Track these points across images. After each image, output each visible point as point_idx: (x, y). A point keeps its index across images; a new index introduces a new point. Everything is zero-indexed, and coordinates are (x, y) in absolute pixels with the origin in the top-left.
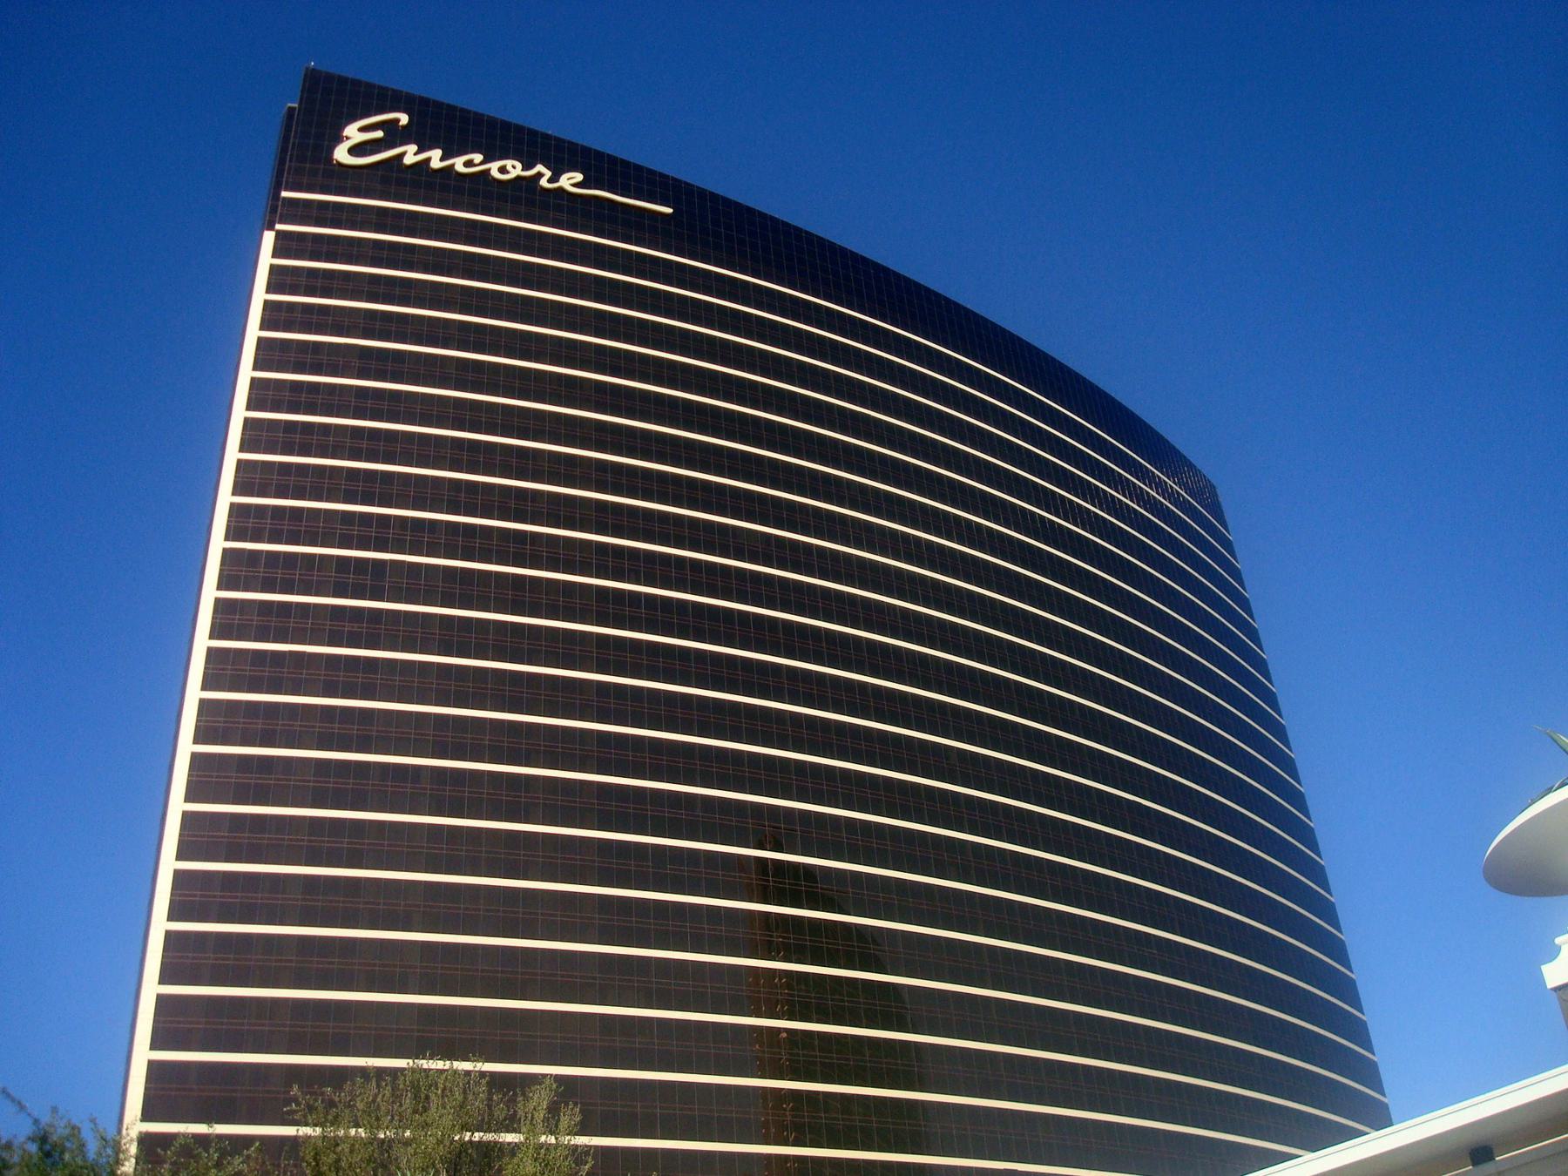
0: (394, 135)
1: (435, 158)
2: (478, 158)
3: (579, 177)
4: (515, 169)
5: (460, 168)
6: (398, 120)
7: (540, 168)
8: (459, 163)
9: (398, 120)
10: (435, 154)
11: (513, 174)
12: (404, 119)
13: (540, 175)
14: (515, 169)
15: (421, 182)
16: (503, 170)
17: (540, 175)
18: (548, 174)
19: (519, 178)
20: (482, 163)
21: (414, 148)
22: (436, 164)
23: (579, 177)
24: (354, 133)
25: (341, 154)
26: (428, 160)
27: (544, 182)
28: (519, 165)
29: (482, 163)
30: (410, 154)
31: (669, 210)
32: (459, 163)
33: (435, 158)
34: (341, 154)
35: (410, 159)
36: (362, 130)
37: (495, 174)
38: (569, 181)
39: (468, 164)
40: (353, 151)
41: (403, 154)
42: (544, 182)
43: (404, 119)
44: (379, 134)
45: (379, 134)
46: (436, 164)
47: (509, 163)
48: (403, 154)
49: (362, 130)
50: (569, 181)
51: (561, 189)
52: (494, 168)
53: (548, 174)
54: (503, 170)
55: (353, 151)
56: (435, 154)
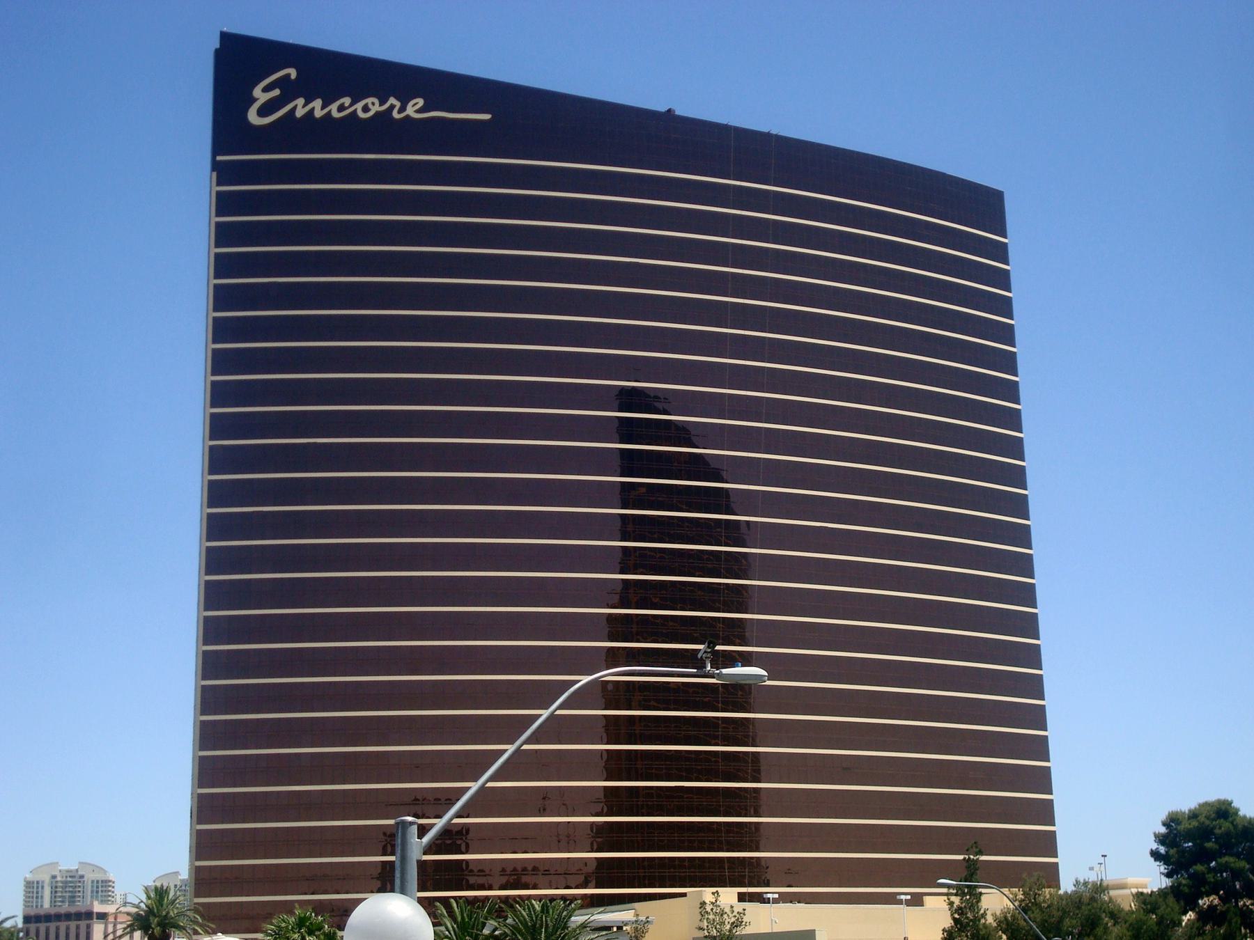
0: (289, 91)
2: (347, 101)
3: (420, 102)
4: (375, 106)
5: (336, 114)
6: (288, 75)
7: (392, 101)
8: (333, 108)
9: (288, 75)
12: (293, 73)
13: (392, 107)
14: (375, 106)
16: (366, 109)
17: (392, 107)
18: (398, 104)
19: (377, 113)
20: (351, 105)
21: (301, 101)
22: (318, 113)
23: (420, 102)
24: (260, 95)
26: (313, 109)
27: (396, 115)
28: (376, 101)
29: (351, 105)
30: (300, 107)
31: (487, 117)
34: (253, 117)
35: (300, 113)
36: (265, 90)
37: (361, 115)
38: (414, 109)
40: (263, 112)
41: (295, 108)
42: (396, 115)
44: (277, 92)
45: (277, 92)
46: (318, 113)
47: (369, 100)
48: (295, 108)
49: (265, 90)
50: (414, 109)
51: (408, 117)
52: (359, 106)
53: (398, 104)
54: (366, 109)
55: (263, 112)
56: (317, 104)
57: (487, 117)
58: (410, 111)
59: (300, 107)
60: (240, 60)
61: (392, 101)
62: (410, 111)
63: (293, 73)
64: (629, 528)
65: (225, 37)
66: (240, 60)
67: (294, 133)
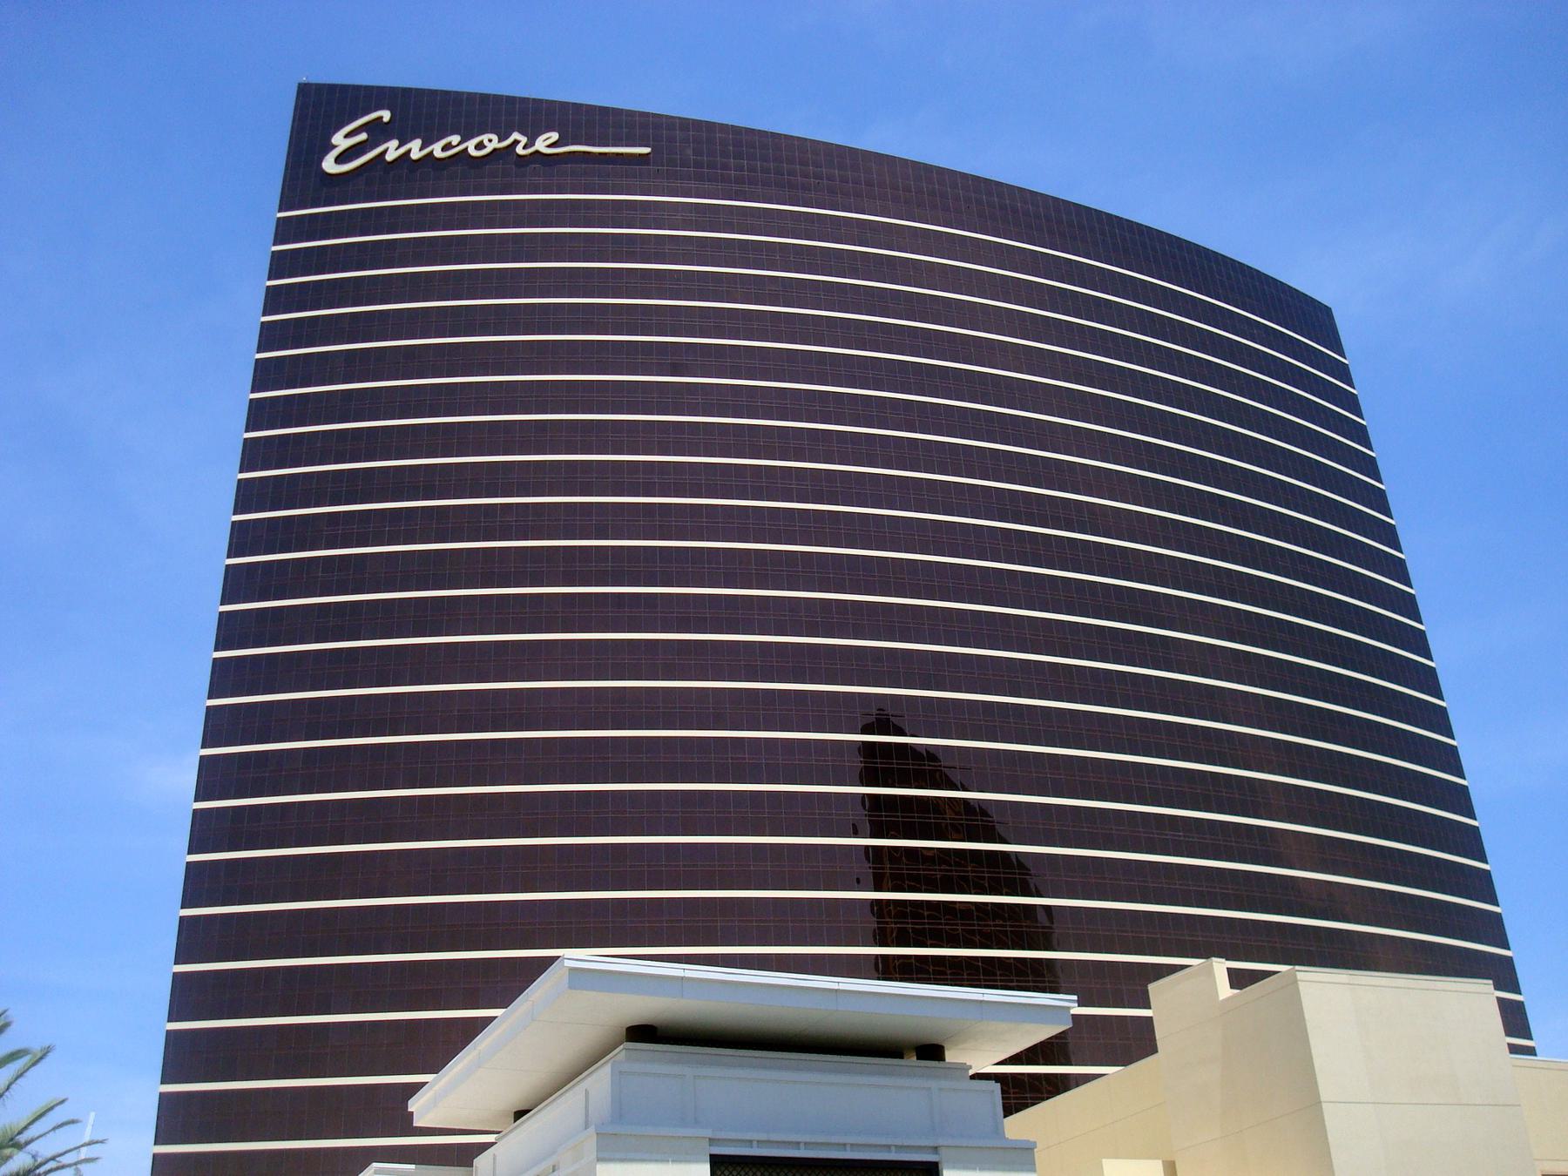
0: (378, 132)
1: (415, 149)
2: (455, 139)
3: (555, 136)
4: (492, 142)
5: (438, 154)
7: (516, 136)
8: (437, 150)
12: (386, 115)
13: (516, 142)
14: (492, 142)
15: (406, 174)
17: (516, 142)
18: (524, 140)
21: (394, 143)
22: (415, 155)
23: (555, 136)
24: (340, 141)
25: (329, 165)
27: (520, 150)
28: (495, 137)
30: (392, 150)
31: (646, 150)
32: (437, 150)
33: (415, 149)
34: (329, 165)
35: (389, 157)
36: (346, 136)
37: (473, 152)
38: (543, 143)
40: (340, 160)
41: (385, 151)
42: (520, 150)
43: (386, 115)
44: (363, 136)
45: (363, 136)
46: (415, 155)
47: (485, 138)
48: (385, 151)
49: (346, 136)
50: (543, 143)
51: (537, 152)
52: (471, 145)
53: (524, 140)
54: (480, 146)
55: (340, 160)
57: (646, 150)
58: (541, 145)
59: (392, 150)
61: (516, 136)
62: (541, 145)
64: (885, 869)
65: (304, 90)
66: (320, 108)
67: (381, 178)
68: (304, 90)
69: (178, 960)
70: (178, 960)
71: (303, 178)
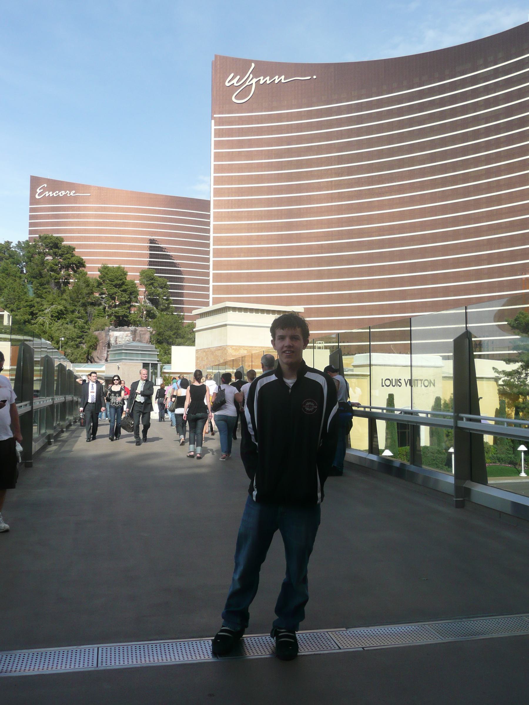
2: (57, 192)
3: (74, 192)
4: (63, 193)
5: (55, 195)
7: (68, 192)
8: (54, 194)
10: (51, 193)
11: (64, 194)
12: (46, 185)
14: (63, 193)
16: (62, 194)
21: (47, 192)
23: (74, 192)
24: (38, 191)
27: (68, 195)
34: (37, 197)
35: (47, 195)
37: (61, 195)
39: (56, 194)
40: (39, 195)
46: (51, 195)
47: (62, 192)
52: (60, 193)
54: (62, 194)
55: (39, 195)
56: (51, 193)
58: (72, 194)
60: (35, 182)
61: (68, 192)
62: (72, 194)
63: (46, 185)
65: (31, 176)
66: (35, 182)
68: (31, 176)
69: (29, 235)
70: (29, 235)
71: (33, 200)
